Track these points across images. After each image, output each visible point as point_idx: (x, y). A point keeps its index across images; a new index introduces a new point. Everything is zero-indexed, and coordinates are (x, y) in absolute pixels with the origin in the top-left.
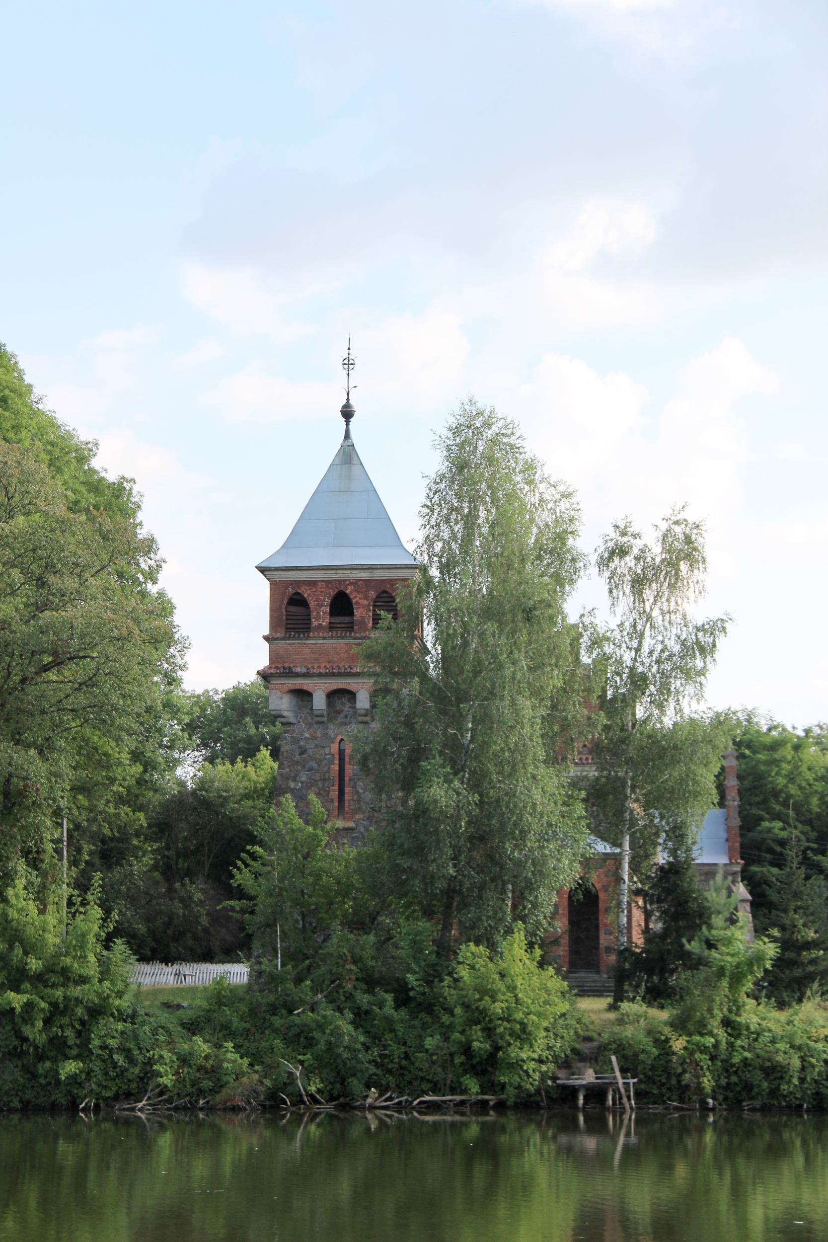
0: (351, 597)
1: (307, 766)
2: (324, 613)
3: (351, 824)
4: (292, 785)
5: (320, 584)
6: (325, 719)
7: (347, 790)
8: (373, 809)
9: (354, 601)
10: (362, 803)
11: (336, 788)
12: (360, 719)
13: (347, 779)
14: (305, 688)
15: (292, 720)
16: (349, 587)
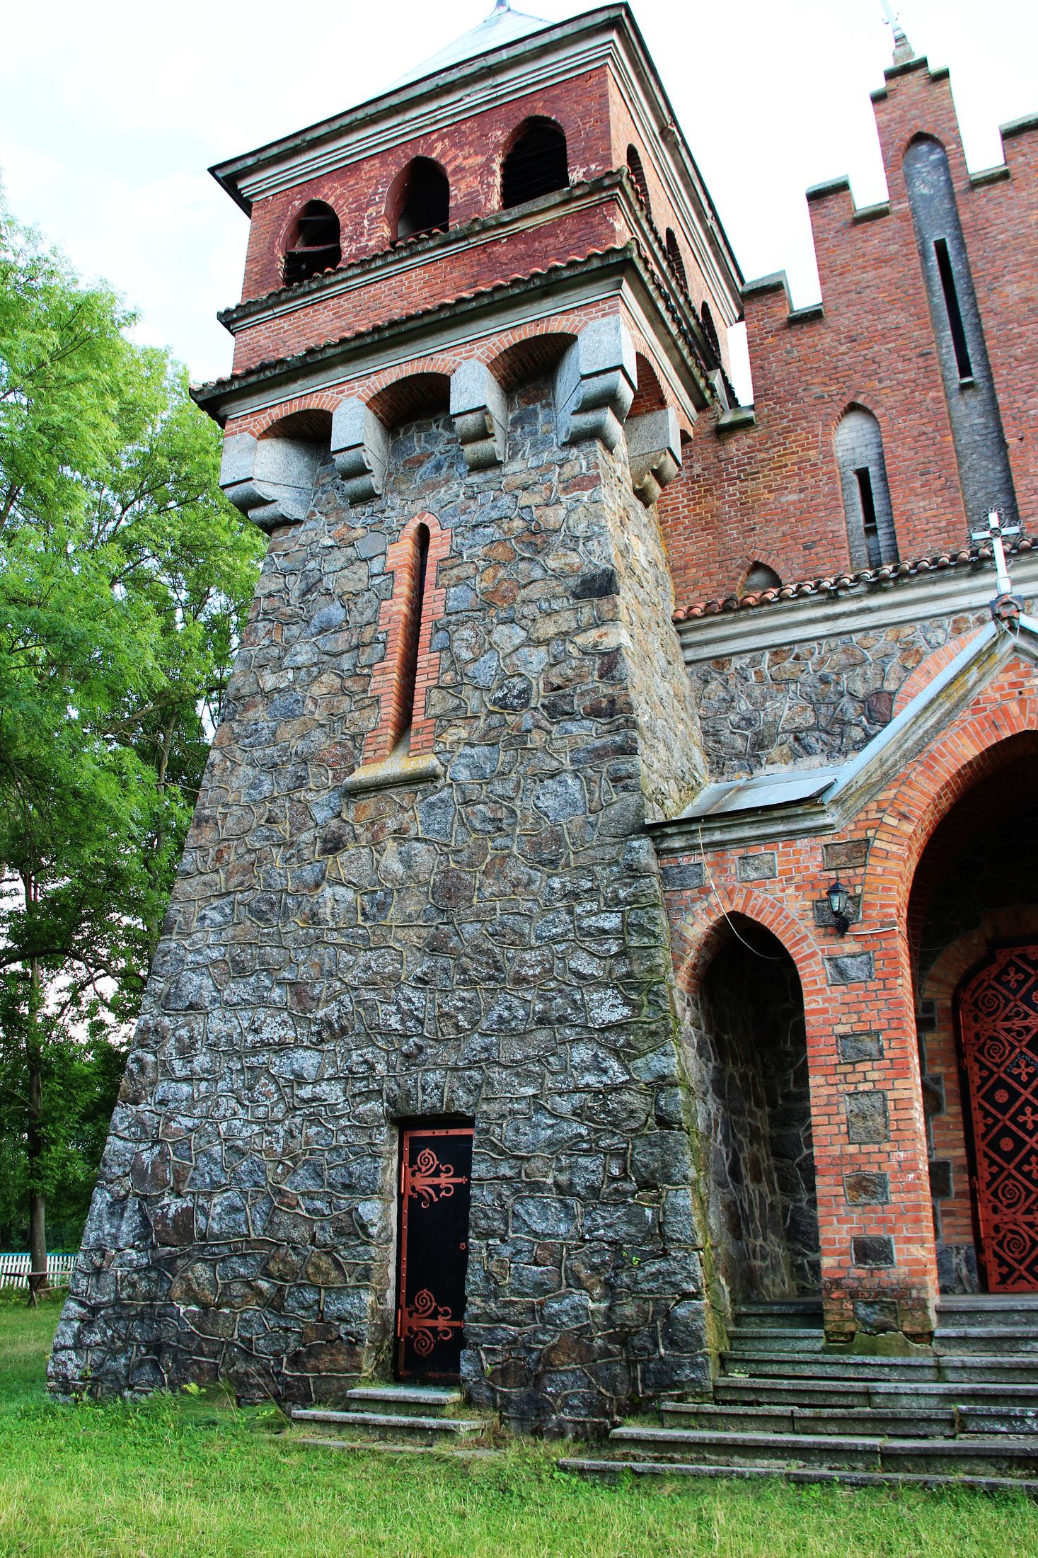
0: (443, 162)
1: (315, 621)
2: (372, 221)
3: (427, 762)
4: (269, 681)
5: (366, 167)
6: (374, 481)
7: (423, 660)
8: (502, 704)
9: (449, 169)
10: (467, 691)
11: (394, 662)
12: (471, 451)
13: (426, 628)
14: (313, 403)
15: (288, 506)
16: (439, 146)
